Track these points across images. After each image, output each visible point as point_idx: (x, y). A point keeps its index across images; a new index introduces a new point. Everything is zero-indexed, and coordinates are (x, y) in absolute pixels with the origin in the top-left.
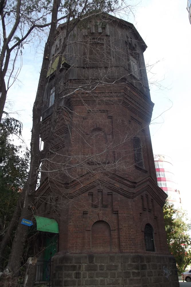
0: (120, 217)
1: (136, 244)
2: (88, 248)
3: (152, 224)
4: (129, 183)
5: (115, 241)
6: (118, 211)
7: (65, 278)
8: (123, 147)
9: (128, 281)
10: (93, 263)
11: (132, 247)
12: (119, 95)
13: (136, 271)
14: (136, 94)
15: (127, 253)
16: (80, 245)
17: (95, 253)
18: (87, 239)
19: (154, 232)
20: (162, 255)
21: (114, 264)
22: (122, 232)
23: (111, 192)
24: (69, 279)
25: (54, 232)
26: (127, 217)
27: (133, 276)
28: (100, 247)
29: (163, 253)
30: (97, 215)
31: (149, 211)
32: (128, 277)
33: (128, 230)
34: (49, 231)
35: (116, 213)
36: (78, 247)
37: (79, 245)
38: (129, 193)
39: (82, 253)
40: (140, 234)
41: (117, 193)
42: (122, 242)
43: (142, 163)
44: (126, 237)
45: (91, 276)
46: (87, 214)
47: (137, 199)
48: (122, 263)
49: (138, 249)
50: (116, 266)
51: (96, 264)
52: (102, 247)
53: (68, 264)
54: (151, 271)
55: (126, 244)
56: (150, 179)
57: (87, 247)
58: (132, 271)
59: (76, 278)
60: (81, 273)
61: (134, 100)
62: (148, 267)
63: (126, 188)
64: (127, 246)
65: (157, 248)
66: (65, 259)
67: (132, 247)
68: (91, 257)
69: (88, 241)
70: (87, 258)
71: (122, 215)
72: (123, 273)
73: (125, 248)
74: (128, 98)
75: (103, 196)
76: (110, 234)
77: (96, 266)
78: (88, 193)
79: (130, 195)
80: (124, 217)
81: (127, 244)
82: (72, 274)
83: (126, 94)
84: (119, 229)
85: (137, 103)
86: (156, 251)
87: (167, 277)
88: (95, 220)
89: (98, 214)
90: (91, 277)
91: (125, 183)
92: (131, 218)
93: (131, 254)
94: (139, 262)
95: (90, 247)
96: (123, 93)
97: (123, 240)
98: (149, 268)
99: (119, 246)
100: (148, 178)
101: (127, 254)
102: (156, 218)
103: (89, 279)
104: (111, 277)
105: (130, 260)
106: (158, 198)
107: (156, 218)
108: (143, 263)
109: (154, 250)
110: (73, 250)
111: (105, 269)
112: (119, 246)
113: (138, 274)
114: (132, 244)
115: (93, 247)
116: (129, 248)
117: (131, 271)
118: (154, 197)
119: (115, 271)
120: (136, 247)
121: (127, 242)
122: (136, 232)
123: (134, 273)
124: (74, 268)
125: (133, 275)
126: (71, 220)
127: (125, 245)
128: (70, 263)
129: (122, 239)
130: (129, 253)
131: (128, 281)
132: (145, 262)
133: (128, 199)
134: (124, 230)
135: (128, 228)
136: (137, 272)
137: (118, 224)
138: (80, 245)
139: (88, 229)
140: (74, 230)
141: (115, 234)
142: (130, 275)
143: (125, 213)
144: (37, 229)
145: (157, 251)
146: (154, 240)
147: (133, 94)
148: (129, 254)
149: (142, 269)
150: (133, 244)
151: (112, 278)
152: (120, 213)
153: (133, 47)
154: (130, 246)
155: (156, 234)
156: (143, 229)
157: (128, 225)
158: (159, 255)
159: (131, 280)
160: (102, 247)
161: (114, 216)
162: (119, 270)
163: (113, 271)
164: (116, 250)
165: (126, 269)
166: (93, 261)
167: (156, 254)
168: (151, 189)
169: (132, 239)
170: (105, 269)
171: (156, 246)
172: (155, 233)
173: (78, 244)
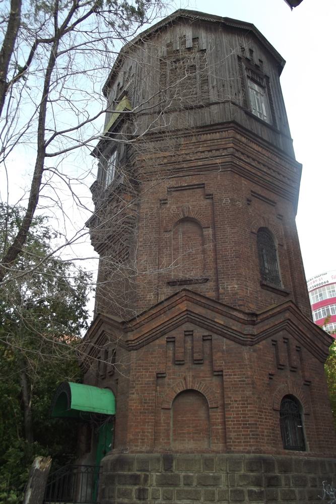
0: (227, 381)
1: (257, 435)
2: (165, 443)
3: (298, 394)
5: (217, 429)
6: (222, 371)
7: (119, 498)
8: (232, 248)
10: (172, 471)
11: (250, 442)
12: (223, 154)
13: (256, 489)
14: (260, 149)
15: (239, 452)
16: (150, 437)
17: (177, 452)
18: (163, 424)
19: (304, 411)
20: (319, 459)
21: (211, 474)
22: (229, 411)
23: (209, 336)
24: (126, 501)
25: (105, 412)
26: (239, 381)
27: (250, 500)
28: (188, 440)
29: (325, 454)
30: (182, 380)
31: (291, 371)
33: (242, 407)
34: (96, 411)
35: (219, 374)
36: (146, 440)
37: (147, 436)
38: (243, 336)
39: (152, 452)
40: (268, 416)
41: (220, 337)
42: (231, 432)
43: (277, 277)
44: (237, 421)
45: (166, 497)
46: (165, 377)
47: (261, 347)
48: (228, 473)
49: (264, 446)
50: (217, 479)
51: (177, 472)
52: (192, 441)
53: (125, 473)
54: (291, 490)
55: (238, 435)
56: (290, 306)
57: (163, 440)
58: (248, 488)
59: (139, 498)
60: (148, 490)
61: (256, 160)
62: (283, 482)
63: (236, 326)
64: (238, 439)
65: (309, 444)
66: (121, 462)
67: (250, 442)
68: (168, 460)
69: (165, 429)
70: (161, 462)
71: (230, 378)
72: (230, 493)
73: (238, 442)
74: (242, 157)
75: (194, 343)
76: (209, 417)
77: (178, 476)
78: (167, 338)
79: (245, 339)
80: (233, 382)
81: (240, 435)
82: (131, 490)
83: (237, 151)
84: (224, 406)
85: (264, 165)
86: (309, 449)
88: (179, 389)
89: (185, 379)
90: (168, 499)
91: (234, 315)
92: (249, 384)
93: (247, 456)
94: (263, 471)
95: (169, 439)
96: (232, 150)
97: (233, 428)
98: (286, 485)
99: (225, 438)
100: (285, 306)
101: (238, 455)
102: (308, 383)
103: (164, 502)
104: (205, 500)
105: (243, 466)
106: (312, 344)
107: (308, 383)
108: (271, 474)
109: (303, 449)
110: (137, 446)
111: (195, 484)
112: (225, 438)
114: (249, 435)
115: (175, 440)
116: (244, 442)
117: (245, 489)
118: (303, 342)
119: (215, 488)
120: (258, 440)
121: (241, 431)
122: (258, 411)
123: (251, 493)
124: (135, 479)
125: (249, 496)
126: (134, 389)
127: (236, 437)
128: (129, 470)
129: (230, 425)
130: (243, 452)
132: (277, 471)
133: (243, 347)
134: (233, 407)
135: (242, 404)
136: (257, 491)
137: (223, 397)
138: (150, 437)
139: (166, 406)
140: (139, 407)
141: (217, 416)
142: (244, 496)
143: (235, 375)
144: (72, 407)
145: (311, 450)
146: (304, 426)
147: (254, 149)
148: (242, 454)
149: (268, 486)
150: (253, 435)
152: (226, 375)
153: (256, 65)
154: (245, 438)
155: (308, 415)
156: (278, 406)
157: (241, 398)
158: (313, 459)
160: (193, 440)
161: (216, 381)
162: (223, 487)
163: (210, 488)
164: (220, 446)
165: (236, 485)
166: (172, 466)
167: (306, 455)
168: (295, 326)
169: (249, 424)
170: (195, 484)
171: (308, 441)
172: (305, 414)
173: (146, 434)
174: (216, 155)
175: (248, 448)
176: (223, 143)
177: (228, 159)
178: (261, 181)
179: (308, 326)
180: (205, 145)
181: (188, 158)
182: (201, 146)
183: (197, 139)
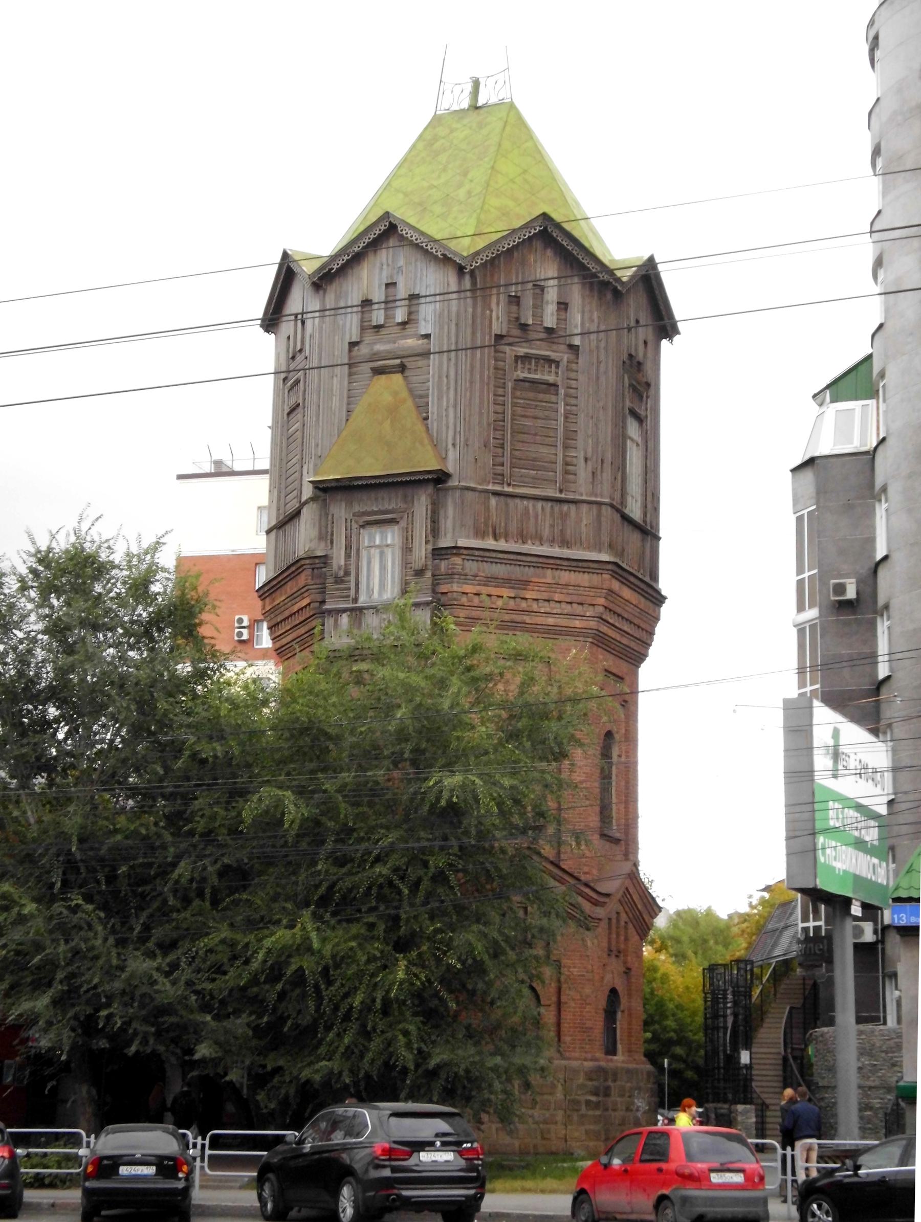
9: (575, 1118)
13: (594, 1099)
15: (576, 1059)
32: (578, 1110)
84: (559, 1004)
87: (639, 1114)
93: (586, 1064)
113: (597, 1106)
123: (588, 1103)
131: (575, 1118)
143: (575, 967)
151: (544, 1112)
159: (583, 1116)
174: (577, 612)
175: (584, 1055)
176: (592, 594)
177: (593, 624)
178: (617, 648)
179: (642, 894)
180: (564, 591)
181: (535, 606)
182: (558, 590)
183: (554, 578)
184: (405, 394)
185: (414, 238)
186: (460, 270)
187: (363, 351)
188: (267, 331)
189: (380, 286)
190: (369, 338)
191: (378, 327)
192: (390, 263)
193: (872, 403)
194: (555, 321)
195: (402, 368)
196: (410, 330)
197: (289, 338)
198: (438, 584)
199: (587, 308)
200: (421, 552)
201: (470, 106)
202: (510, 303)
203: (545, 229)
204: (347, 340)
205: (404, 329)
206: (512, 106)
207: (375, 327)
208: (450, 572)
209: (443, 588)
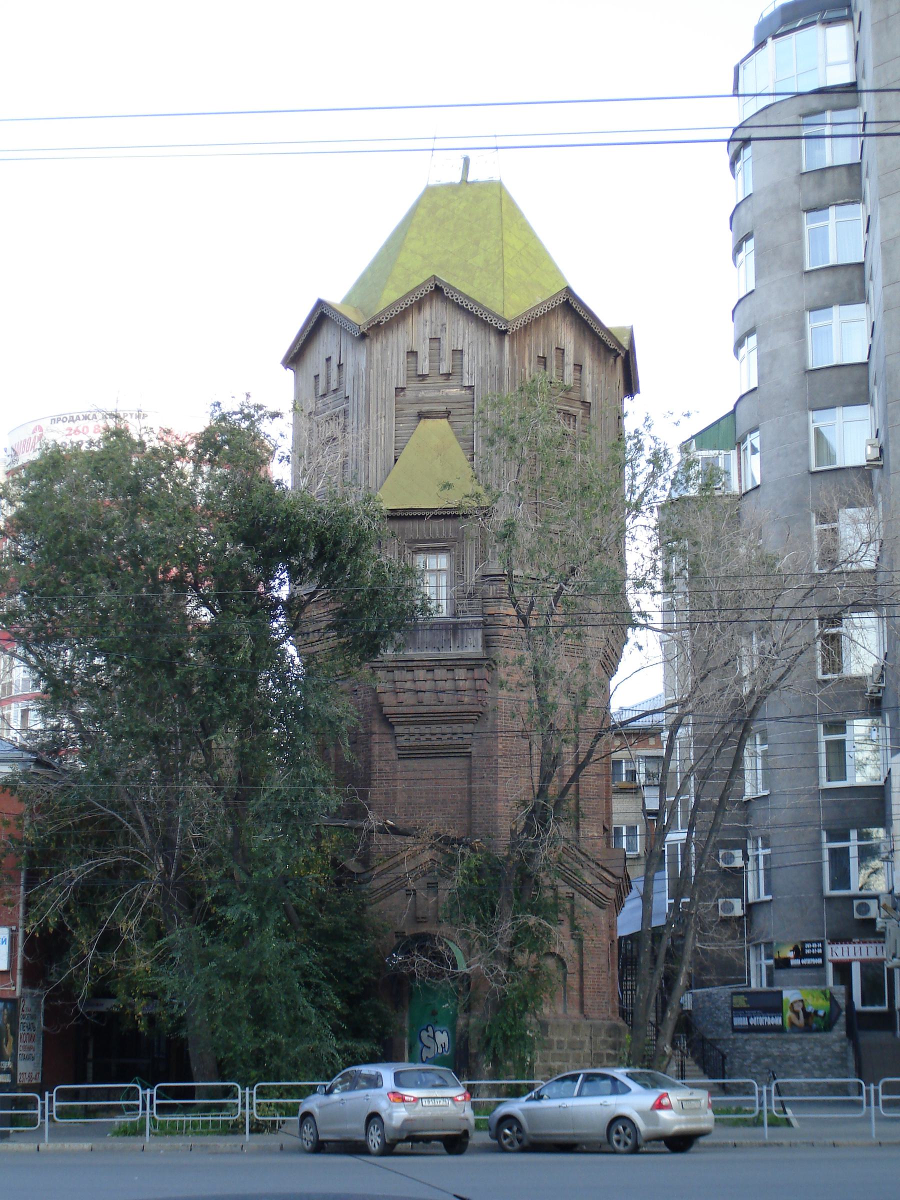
4: (610, 878)
50: (582, 1043)
51: (551, 1037)
99: (582, 1004)
123: (609, 1055)
162: (587, 1050)
163: (577, 1051)
164: (575, 1012)
184: (452, 437)
185: (459, 301)
186: (502, 333)
187: (410, 394)
188: (286, 368)
189: (424, 339)
190: (414, 384)
191: (423, 377)
192: (434, 319)
193: (733, 453)
194: (572, 381)
195: (447, 414)
196: (454, 381)
197: (317, 377)
198: (486, 606)
199: (596, 371)
200: (472, 576)
201: (462, 180)
202: (539, 362)
203: (568, 300)
204: (395, 386)
205: (448, 379)
206: (500, 186)
207: (420, 376)
208: (498, 596)
209: (491, 610)
